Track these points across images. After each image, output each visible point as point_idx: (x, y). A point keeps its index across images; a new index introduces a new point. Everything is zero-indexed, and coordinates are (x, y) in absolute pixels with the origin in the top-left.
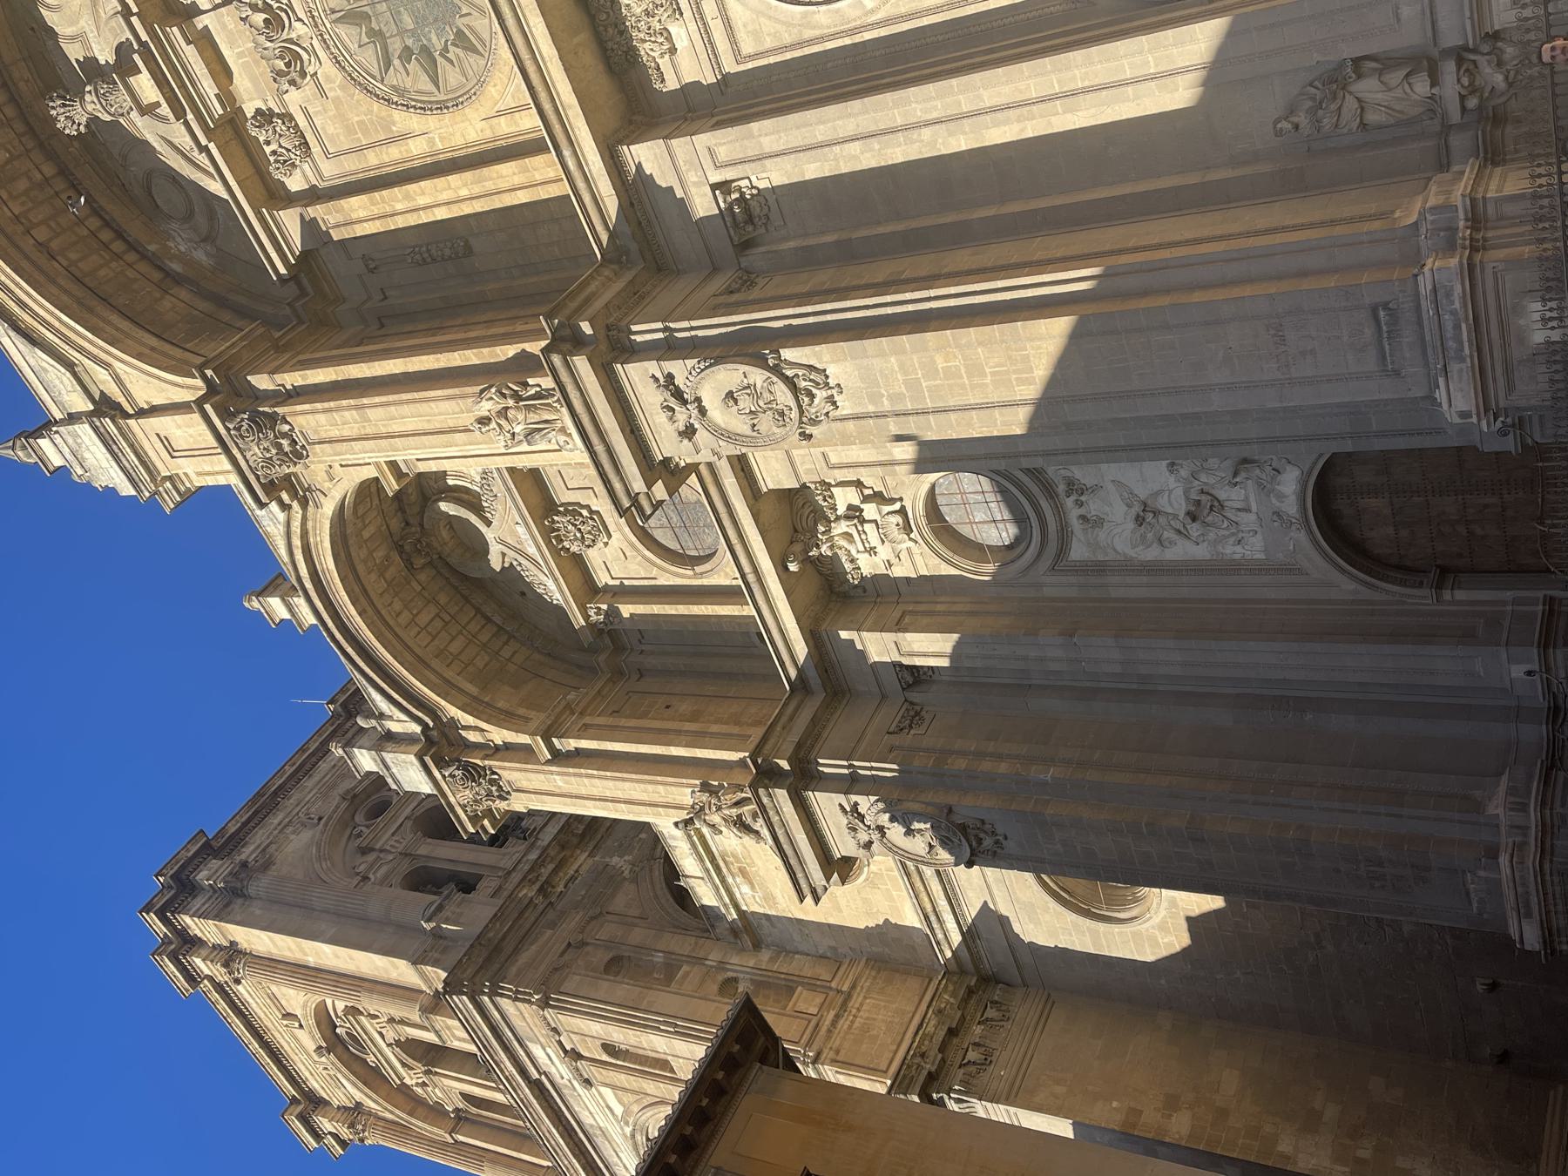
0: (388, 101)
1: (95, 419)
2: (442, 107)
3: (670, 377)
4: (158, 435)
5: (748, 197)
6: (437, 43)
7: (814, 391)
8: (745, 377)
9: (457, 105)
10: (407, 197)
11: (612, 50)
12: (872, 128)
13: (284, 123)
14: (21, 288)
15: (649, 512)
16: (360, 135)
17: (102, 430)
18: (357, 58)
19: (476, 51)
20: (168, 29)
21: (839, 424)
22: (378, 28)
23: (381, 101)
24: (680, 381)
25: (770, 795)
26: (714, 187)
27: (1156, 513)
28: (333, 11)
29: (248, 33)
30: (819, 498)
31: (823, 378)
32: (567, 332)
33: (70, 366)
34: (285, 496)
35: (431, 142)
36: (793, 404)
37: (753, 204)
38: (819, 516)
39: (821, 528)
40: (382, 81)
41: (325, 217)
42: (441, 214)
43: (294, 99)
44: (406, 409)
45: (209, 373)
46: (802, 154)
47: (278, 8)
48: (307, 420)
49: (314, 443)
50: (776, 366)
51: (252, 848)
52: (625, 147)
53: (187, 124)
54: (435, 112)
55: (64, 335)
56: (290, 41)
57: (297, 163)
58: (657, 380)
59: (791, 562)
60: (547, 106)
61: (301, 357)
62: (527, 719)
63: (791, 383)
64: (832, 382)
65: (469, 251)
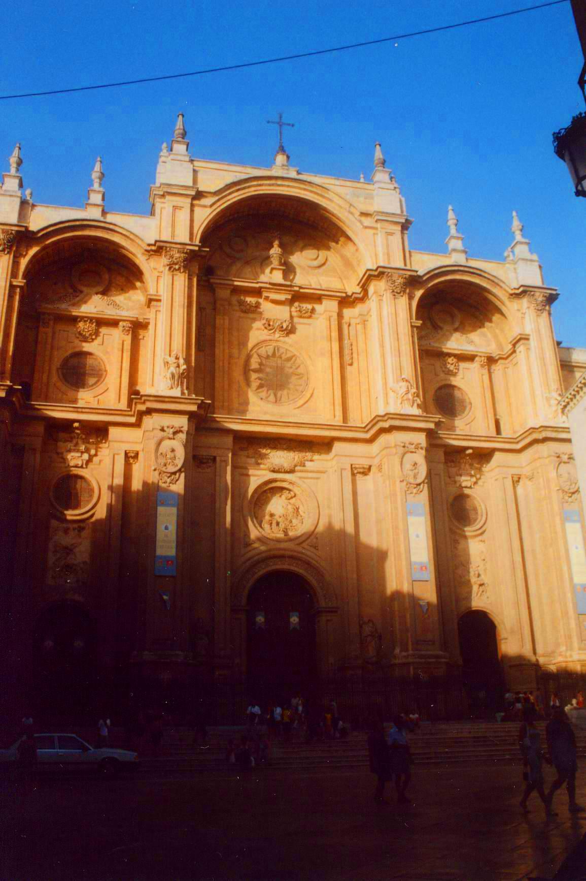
1: (196, 190)
4: (183, 207)
6: (261, 375)
19: (257, 389)
25: (3, 389)
27: (68, 554)
28: (278, 349)
32: (203, 405)
34: (154, 248)
37: (204, 466)
39: (84, 437)
40: (255, 352)
48: (181, 280)
53: (266, 283)
56: (275, 331)
57: (241, 307)
60: (253, 422)
63: (175, 473)
64: (171, 485)
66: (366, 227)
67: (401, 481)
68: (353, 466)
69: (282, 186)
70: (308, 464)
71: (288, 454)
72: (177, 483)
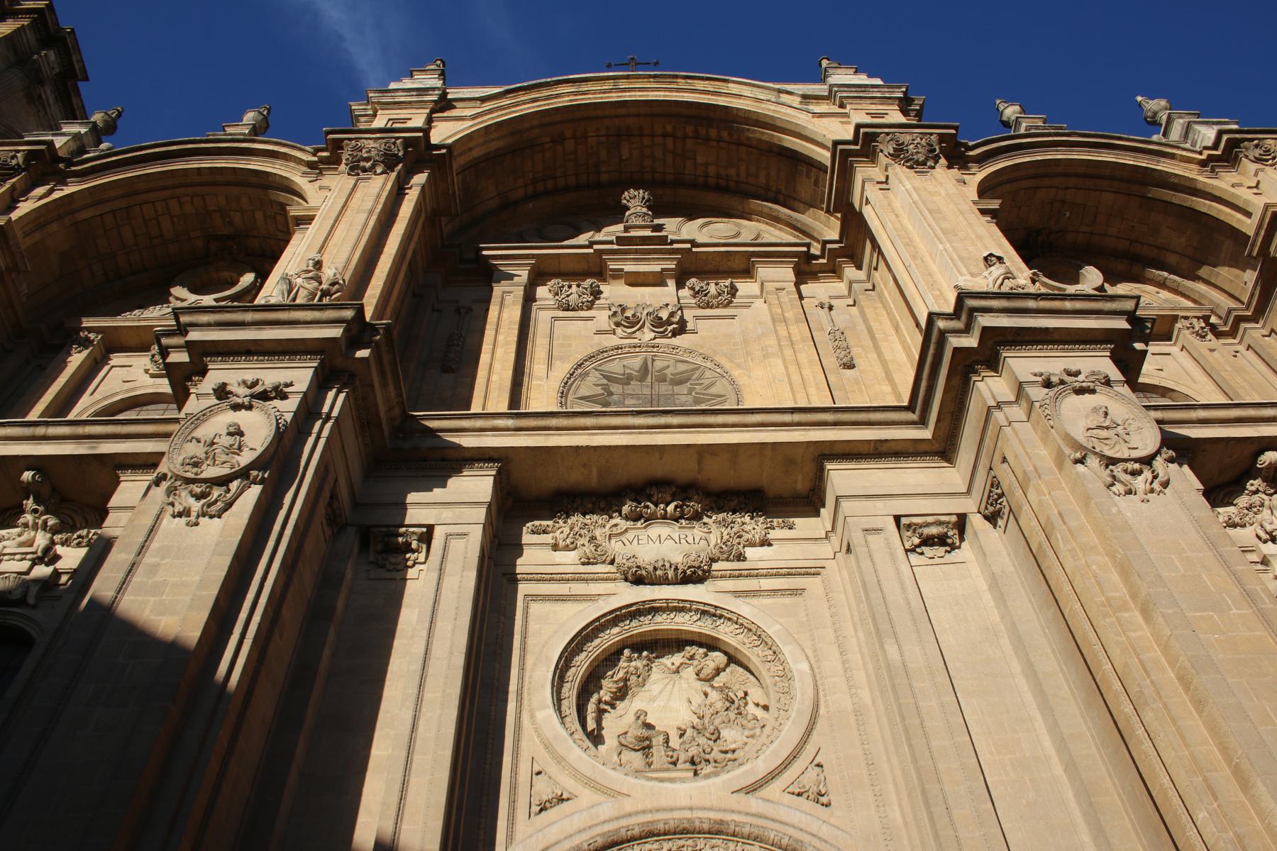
0: (580, 365)
1: (440, 92)
2: (563, 395)
3: (284, 396)
4: (410, 119)
5: (408, 556)
7: (203, 501)
8: (251, 449)
9: (561, 403)
10: (507, 343)
11: (573, 502)
12: (431, 670)
13: (588, 301)
14: (545, 105)
15: (164, 341)
16: (561, 342)
17: (431, 92)
18: (616, 362)
20: (675, 263)
21: (155, 512)
22: (632, 382)
23: (581, 361)
24: (277, 403)
26: (430, 528)
28: (653, 360)
29: (657, 305)
30: (84, 532)
31: (213, 513)
33: (483, 100)
35: (540, 379)
36: (203, 476)
37: (400, 559)
38: (66, 527)
39: (52, 521)
41: (512, 295)
42: (485, 358)
43: (602, 317)
44: (355, 234)
45: (444, 151)
46: (431, 603)
47: (666, 330)
48: (377, 186)
49: (357, 181)
50: (248, 478)
51: (52, 102)
52: (494, 473)
53: (611, 242)
54: (561, 388)
55: (504, 109)
57: (557, 297)
58: (287, 385)
59: (34, 476)
60: (554, 422)
61: (423, 215)
62: (26, 234)
63: (223, 481)
64: (204, 521)
65: (447, 369)
66: (821, 115)
67: (1077, 461)
68: (904, 521)
69: (630, 90)
70: (750, 552)
71: (689, 532)
72: (225, 515)
